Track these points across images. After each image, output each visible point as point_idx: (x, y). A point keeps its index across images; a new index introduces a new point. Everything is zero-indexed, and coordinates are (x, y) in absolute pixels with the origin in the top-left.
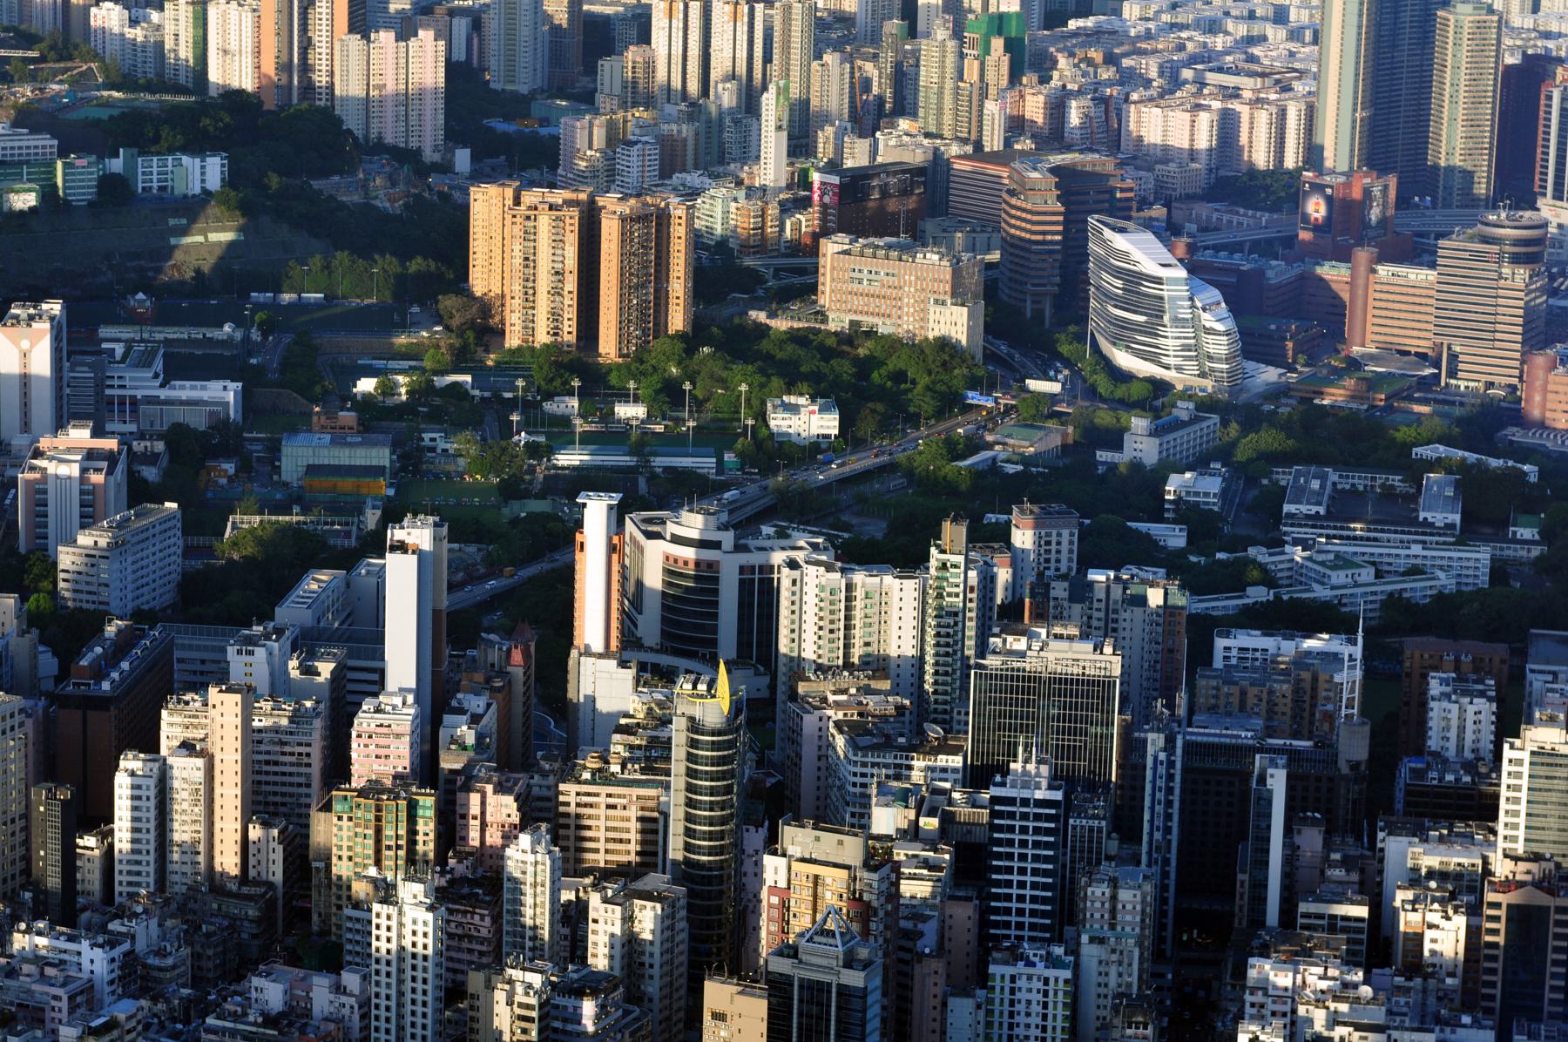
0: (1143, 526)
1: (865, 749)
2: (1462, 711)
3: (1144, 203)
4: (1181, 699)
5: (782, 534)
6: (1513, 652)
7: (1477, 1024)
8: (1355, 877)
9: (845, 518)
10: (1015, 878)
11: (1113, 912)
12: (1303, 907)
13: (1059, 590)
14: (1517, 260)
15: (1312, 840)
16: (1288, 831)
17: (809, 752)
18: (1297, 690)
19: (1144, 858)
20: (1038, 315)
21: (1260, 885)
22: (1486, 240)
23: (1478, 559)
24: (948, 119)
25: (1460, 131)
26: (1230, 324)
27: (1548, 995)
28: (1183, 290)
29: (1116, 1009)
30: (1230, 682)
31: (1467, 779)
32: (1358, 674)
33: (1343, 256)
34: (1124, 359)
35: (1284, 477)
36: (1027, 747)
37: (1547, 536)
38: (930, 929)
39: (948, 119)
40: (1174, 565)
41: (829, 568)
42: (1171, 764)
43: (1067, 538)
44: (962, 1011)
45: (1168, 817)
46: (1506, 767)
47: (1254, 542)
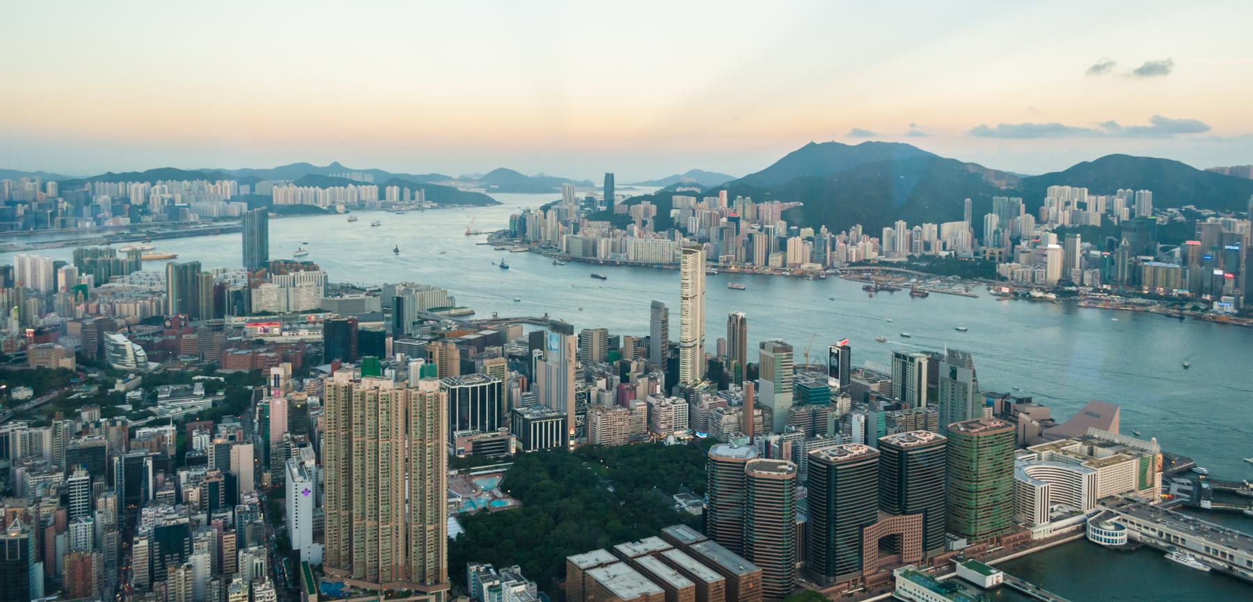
1: (34, 476)
3: (122, 327)
5: (15, 423)
6: (215, 422)
7: (202, 513)
8: (173, 483)
9: (35, 416)
10: (77, 501)
12: (158, 493)
13: (92, 426)
15: (161, 476)
16: (154, 475)
17: (18, 479)
18: (158, 440)
20: (92, 358)
21: (147, 491)
23: (209, 401)
24: (66, 311)
25: (204, 302)
29: (105, 529)
30: (139, 441)
34: (115, 366)
35: (159, 389)
36: (78, 467)
37: (226, 394)
38: (51, 520)
39: (66, 311)
40: (128, 415)
41: (24, 430)
42: (121, 464)
43: (96, 413)
44: (61, 539)
45: (121, 477)
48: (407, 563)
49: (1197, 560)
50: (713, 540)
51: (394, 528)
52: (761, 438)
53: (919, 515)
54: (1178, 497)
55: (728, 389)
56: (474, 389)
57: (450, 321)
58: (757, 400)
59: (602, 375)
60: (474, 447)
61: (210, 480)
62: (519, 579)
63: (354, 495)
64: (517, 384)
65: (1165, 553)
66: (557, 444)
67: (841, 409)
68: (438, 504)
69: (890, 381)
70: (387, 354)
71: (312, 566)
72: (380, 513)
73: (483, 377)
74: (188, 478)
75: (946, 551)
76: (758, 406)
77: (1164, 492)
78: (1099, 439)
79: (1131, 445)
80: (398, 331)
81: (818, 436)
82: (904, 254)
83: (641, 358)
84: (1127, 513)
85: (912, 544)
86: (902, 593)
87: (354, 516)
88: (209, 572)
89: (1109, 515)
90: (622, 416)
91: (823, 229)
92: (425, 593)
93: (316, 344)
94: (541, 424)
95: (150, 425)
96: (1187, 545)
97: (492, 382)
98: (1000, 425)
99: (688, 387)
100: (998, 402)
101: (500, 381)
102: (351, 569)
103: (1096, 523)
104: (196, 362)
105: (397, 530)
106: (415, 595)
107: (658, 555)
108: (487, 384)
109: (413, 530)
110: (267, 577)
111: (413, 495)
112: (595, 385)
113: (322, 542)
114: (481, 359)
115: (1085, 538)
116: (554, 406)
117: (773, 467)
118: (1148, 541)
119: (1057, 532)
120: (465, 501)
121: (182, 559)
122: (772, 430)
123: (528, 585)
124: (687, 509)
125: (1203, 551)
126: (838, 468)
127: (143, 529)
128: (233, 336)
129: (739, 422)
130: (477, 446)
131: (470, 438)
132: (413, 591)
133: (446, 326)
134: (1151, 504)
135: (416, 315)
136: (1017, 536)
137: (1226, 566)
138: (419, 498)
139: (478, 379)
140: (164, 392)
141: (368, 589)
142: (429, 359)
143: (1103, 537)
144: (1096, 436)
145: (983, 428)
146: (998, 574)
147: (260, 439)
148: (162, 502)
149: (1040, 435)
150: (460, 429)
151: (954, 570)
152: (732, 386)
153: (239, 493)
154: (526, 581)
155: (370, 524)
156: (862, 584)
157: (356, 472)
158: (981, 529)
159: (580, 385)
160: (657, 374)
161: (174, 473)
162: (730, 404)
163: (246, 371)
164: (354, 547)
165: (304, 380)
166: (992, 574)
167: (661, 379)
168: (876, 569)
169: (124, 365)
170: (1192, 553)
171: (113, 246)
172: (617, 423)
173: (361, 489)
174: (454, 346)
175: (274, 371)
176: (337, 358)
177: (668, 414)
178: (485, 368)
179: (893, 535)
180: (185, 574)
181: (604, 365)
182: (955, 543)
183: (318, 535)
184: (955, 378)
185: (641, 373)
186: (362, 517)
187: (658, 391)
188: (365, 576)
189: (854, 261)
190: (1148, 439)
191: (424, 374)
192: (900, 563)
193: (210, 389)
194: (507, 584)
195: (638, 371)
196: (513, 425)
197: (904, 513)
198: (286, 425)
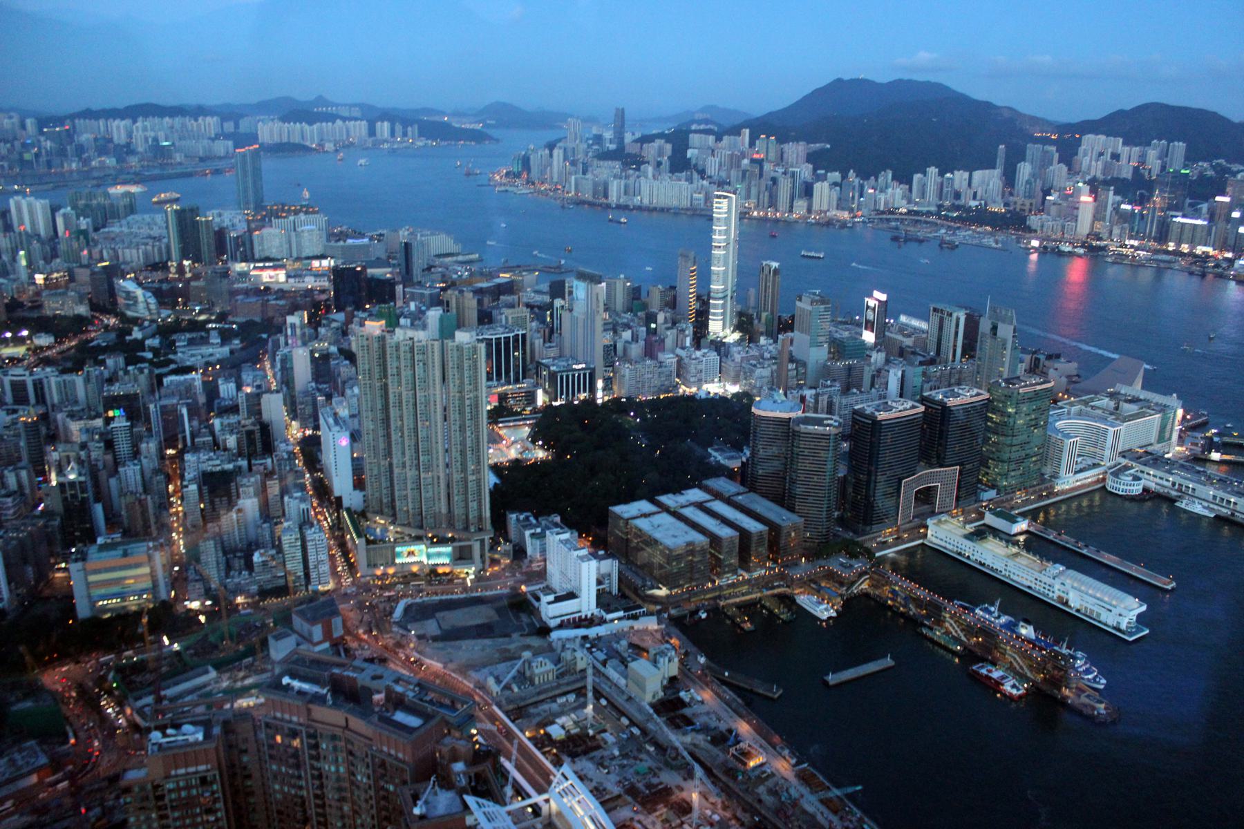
56: (498, 340)
59: (627, 326)
64: (539, 335)
83: (667, 309)
94: (568, 377)
97: (516, 332)
108: (511, 335)
112: (621, 337)
116: (580, 358)
130: (503, 397)
131: (494, 391)
139: (501, 330)
160: (684, 326)
167: (690, 331)
172: (646, 376)
181: (629, 315)
185: (670, 325)
195: (666, 321)
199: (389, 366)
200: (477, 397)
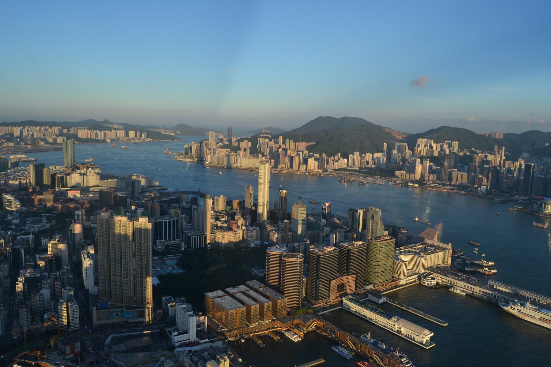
0: (10, 226)
2: (45, 241)
4: (11, 244)
7: (46, 272)
11: (4, 268)
12: (26, 264)
14: (52, 194)
15: (28, 257)
16: (25, 256)
19: (8, 262)
22: (48, 192)
23: (48, 225)
26: (20, 203)
27: (54, 268)
28: (14, 200)
29: (4, 278)
31: (45, 248)
32: (32, 238)
33: (33, 195)
34: (8, 208)
40: (13, 230)
46: (48, 246)
47: (23, 226)
48: (135, 295)
49: (461, 291)
50: (268, 287)
51: (129, 280)
52: (291, 244)
53: (354, 275)
54: (457, 266)
55: (278, 223)
56: (166, 222)
57: (156, 192)
58: (290, 228)
60: (165, 247)
61: (49, 259)
62: (184, 303)
63: (111, 266)
64: (185, 220)
65: (450, 288)
66: (202, 246)
67: (326, 232)
68: (148, 271)
69: (347, 220)
70: (127, 206)
71: (94, 296)
72: (123, 274)
73: (170, 217)
74: (40, 258)
75: (364, 290)
76: (290, 231)
77: (451, 265)
78: (429, 244)
79: (441, 246)
80: (133, 196)
81: (315, 243)
82: (358, 167)
84: (437, 273)
85: (351, 288)
86: (346, 306)
87: (111, 275)
88: (49, 297)
89: (430, 274)
90: (231, 235)
91: (324, 155)
92: (143, 308)
93: (96, 201)
94: (195, 238)
95: (23, 234)
96: (458, 285)
97: (173, 219)
98: (389, 238)
99: (260, 222)
100: (391, 229)
101: (177, 219)
102: (111, 297)
103: (425, 277)
104: (43, 208)
105: (130, 280)
106: (139, 309)
107: (244, 293)
109: (137, 282)
110: (74, 300)
111: (137, 267)
113: (98, 286)
114: (169, 209)
115: (420, 283)
117: (294, 256)
118: (444, 284)
119: (410, 281)
120: (161, 270)
121: (38, 291)
122: (296, 241)
123: (188, 305)
124: (258, 274)
125: (464, 287)
126: (322, 256)
127: (20, 279)
128: (59, 197)
129: (282, 238)
130: (167, 247)
132: (138, 307)
133: (154, 194)
134: (446, 269)
135: (141, 189)
136: (393, 283)
137: (471, 293)
138: (139, 268)
140: (29, 221)
141: (118, 306)
142: (146, 209)
143: (427, 282)
144: (428, 243)
145: (383, 239)
146: (384, 298)
147: (71, 242)
148: (28, 267)
149: (406, 242)
150: (159, 239)
151: (367, 297)
152: (280, 222)
153: (62, 265)
154: (187, 303)
155: (118, 278)
156: (329, 303)
157: (112, 257)
158: (379, 280)
159: (213, 221)
161: (34, 256)
162: (279, 230)
163: (65, 212)
164: (112, 288)
165: (91, 217)
166: (382, 298)
167: (249, 218)
168: (336, 297)
169: (11, 208)
170: (460, 288)
171: (7, 156)
173: (114, 264)
174: (157, 202)
175: (77, 212)
176: (105, 207)
177: (252, 234)
178: (171, 213)
179: (344, 284)
180: (39, 298)
182: (368, 286)
183: (96, 283)
184: (373, 219)
186: (115, 276)
187: (248, 224)
188: (117, 300)
189: (336, 168)
190: (448, 244)
191: (143, 215)
192: (345, 295)
193: (49, 220)
194: (178, 304)
196: (183, 238)
197: (348, 275)
198: (82, 236)
199: (110, 232)
200: (148, 245)
